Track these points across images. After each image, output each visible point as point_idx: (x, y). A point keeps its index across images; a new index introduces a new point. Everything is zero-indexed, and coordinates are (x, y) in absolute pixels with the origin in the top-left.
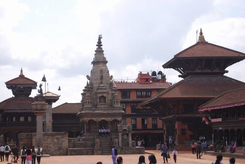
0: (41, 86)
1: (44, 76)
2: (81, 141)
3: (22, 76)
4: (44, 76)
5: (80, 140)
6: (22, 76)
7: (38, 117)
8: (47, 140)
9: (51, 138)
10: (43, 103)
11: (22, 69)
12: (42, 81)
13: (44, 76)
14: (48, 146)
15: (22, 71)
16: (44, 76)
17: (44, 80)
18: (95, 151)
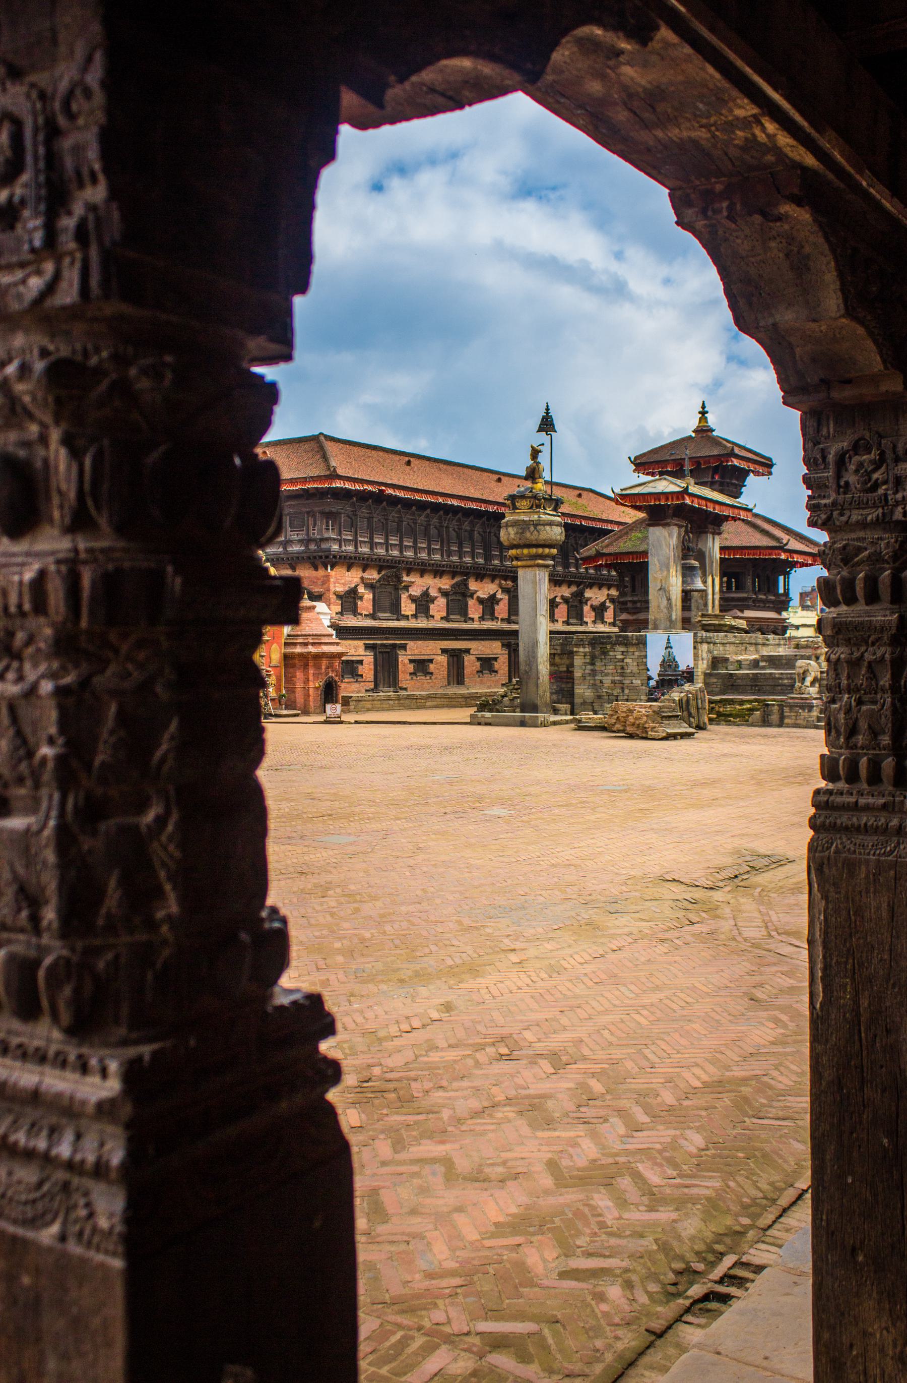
0: (535, 453)
1: (547, 409)
2: (763, 668)
3: (703, 431)
4: (547, 409)
5: (761, 664)
6: (703, 431)
7: (521, 572)
8: (622, 660)
9: (637, 653)
10: (527, 519)
11: (703, 407)
12: (540, 430)
13: (547, 413)
14: (627, 682)
15: (703, 413)
16: (547, 413)
17: (547, 425)
18: (786, 709)
